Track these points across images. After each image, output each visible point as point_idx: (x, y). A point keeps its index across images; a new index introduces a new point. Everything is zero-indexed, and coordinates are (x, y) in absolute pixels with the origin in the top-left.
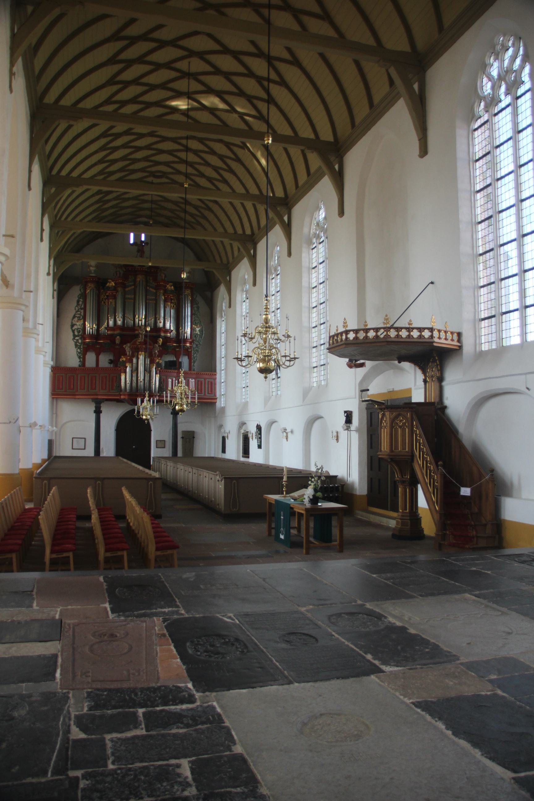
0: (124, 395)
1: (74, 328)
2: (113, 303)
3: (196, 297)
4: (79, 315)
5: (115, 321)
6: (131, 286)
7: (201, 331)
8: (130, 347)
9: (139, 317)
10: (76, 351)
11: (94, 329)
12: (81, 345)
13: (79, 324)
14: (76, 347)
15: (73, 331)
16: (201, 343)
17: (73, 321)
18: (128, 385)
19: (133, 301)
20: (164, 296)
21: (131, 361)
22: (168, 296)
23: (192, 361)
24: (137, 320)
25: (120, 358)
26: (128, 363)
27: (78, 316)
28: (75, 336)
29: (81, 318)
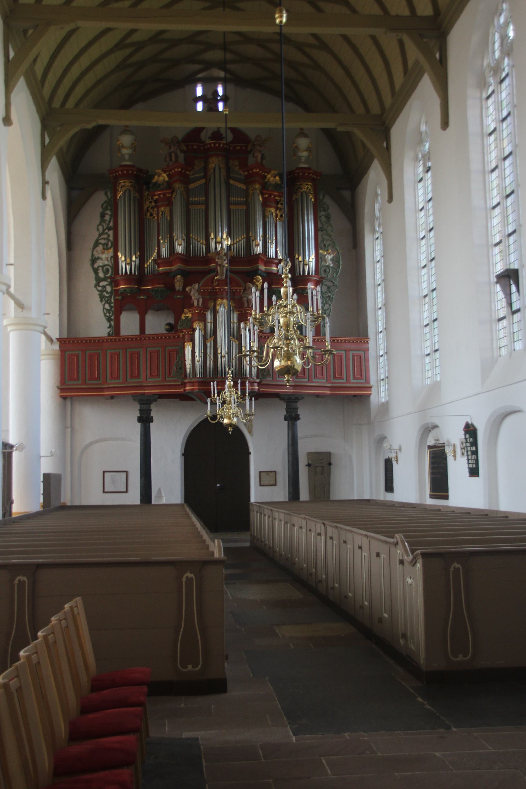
0: (193, 384)
1: (96, 266)
2: (167, 213)
3: (324, 196)
7: (336, 260)
8: (199, 291)
9: (216, 237)
10: (102, 307)
11: (133, 264)
12: (110, 297)
13: (105, 258)
14: (101, 301)
15: (96, 271)
16: (336, 283)
17: (95, 253)
18: (198, 365)
19: (203, 207)
20: (262, 194)
21: (203, 319)
22: (270, 195)
24: (213, 245)
25: (183, 312)
26: (197, 322)
27: (103, 241)
28: (98, 280)
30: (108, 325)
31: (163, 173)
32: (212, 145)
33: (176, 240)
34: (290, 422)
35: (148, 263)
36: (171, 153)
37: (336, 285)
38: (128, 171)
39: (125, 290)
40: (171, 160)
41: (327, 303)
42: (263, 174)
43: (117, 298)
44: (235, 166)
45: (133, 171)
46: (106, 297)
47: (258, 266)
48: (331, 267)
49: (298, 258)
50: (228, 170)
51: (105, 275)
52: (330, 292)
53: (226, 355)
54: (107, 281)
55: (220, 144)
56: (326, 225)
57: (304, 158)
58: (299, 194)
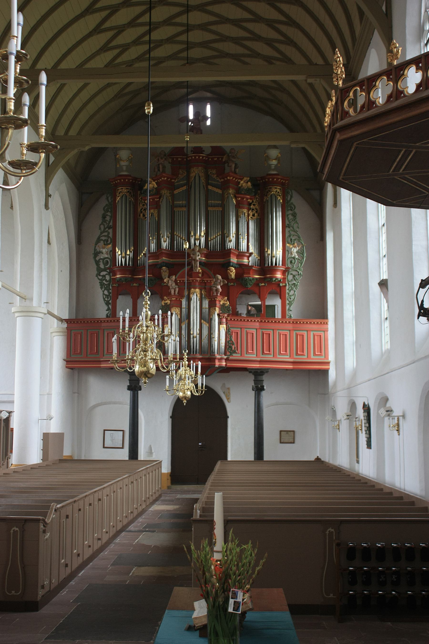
1: (97, 259)
2: (156, 215)
3: (291, 197)
4: (106, 238)
5: (159, 244)
6: (182, 186)
8: (176, 281)
10: (102, 293)
11: (128, 257)
12: (109, 284)
13: (105, 252)
14: (101, 288)
15: (97, 263)
17: (97, 248)
20: (236, 197)
22: (242, 198)
23: (287, 302)
26: (174, 308)
27: (103, 238)
28: (99, 270)
29: (109, 240)
30: (106, 308)
31: (153, 181)
32: (193, 158)
33: (162, 237)
34: (256, 392)
35: (141, 256)
36: (159, 165)
37: (300, 274)
38: (124, 180)
39: (120, 279)
40: (159, 170)
41: (292, 290)
42: (237, 180)
43: (114, 285)
44: (213, 174)
45: (129, 180)
46: (106, 285)
47: (230, 259)
48: (297, 259)
49: (267, 251)
50: (207, 177)
51: (105, 266)
52: (295, 280)
53: (198, 336)
54: (107, 272)
55: (199, 156)
56: (293, 222)
57: (274, 166)
58: (269, 196)
